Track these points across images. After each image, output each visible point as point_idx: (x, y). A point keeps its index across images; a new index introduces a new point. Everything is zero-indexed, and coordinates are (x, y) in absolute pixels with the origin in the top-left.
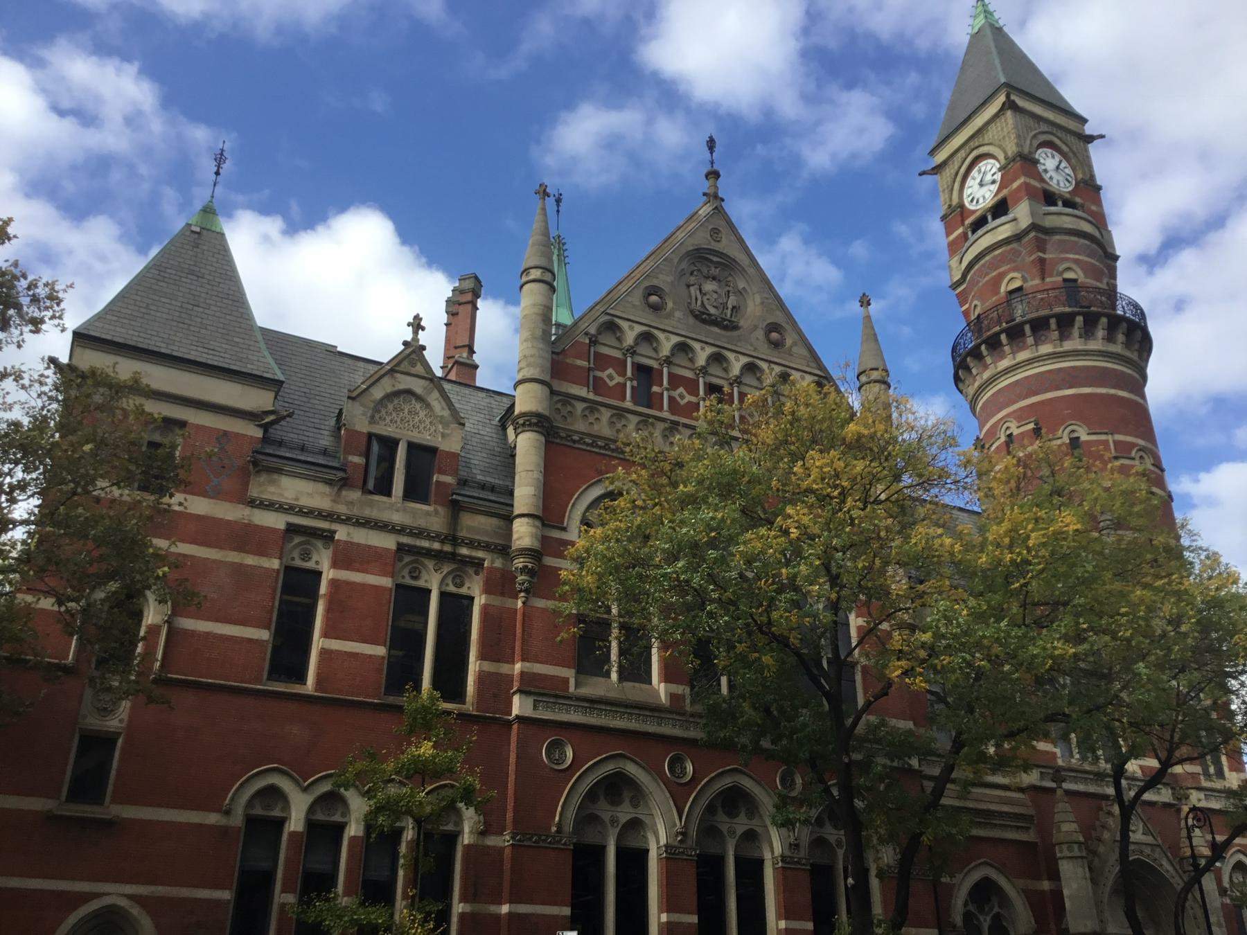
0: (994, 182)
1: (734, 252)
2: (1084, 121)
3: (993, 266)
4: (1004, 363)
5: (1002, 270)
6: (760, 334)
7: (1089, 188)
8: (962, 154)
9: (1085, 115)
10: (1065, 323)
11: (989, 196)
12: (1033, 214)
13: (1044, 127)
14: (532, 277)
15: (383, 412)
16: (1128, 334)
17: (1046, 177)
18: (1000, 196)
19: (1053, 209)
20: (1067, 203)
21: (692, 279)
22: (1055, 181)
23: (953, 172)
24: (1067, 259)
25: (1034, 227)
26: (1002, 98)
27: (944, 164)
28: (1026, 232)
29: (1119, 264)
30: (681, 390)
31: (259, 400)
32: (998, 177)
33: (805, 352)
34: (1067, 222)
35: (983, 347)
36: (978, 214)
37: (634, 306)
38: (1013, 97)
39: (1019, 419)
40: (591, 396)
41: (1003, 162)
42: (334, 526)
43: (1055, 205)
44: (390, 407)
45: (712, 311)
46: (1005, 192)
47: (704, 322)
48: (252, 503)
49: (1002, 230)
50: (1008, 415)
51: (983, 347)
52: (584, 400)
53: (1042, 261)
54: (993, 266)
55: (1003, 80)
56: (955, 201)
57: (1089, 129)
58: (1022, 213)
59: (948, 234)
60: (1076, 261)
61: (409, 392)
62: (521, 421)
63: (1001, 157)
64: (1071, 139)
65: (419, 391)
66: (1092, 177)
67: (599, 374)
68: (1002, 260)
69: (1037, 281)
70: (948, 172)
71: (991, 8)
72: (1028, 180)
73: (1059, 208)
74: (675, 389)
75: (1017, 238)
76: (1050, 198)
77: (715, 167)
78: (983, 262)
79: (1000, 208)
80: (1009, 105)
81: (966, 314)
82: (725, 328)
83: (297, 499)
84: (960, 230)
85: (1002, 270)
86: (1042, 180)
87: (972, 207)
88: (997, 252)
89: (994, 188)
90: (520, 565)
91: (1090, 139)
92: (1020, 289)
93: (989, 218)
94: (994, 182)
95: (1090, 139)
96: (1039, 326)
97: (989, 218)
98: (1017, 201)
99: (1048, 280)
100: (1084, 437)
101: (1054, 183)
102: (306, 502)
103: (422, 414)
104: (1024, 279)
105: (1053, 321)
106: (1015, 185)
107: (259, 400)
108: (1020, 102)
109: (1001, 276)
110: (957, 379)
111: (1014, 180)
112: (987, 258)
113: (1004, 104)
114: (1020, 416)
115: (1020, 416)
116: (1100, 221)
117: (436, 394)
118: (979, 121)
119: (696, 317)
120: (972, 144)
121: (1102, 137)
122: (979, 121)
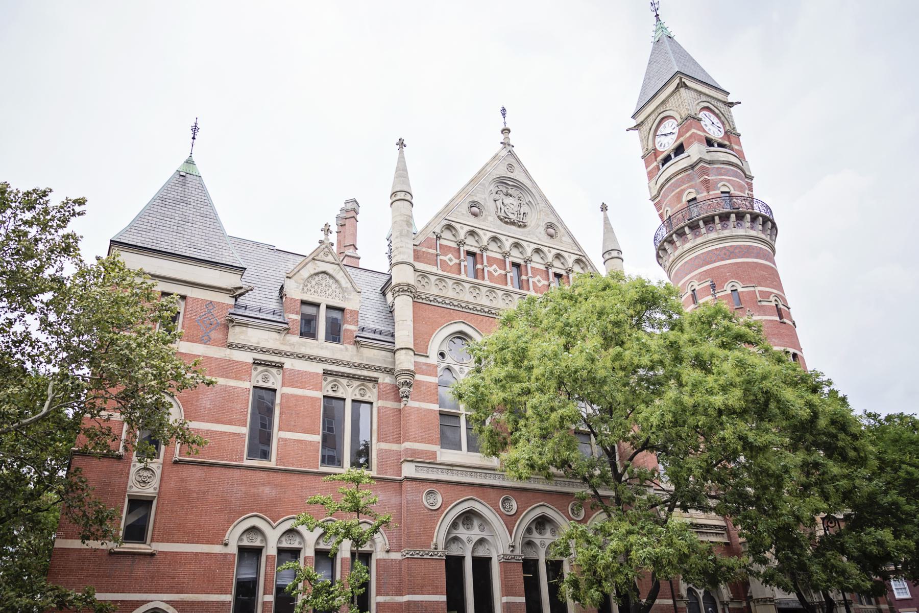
1: (522, 178)
3: (677, 185)
4: (688, 246)
6: (542, 229)
7: (732, 135)
8: (653, 117)
10: (725, 217)
11: (671, 142)
12: (700, 152)
13: (704, 98)
14: (398, 198)
15: (309, 286)
16: (764, 223)
17: (706, 129)
19: (712, 149)
20: (720, 145)
21: (497, 196)
23: (648, 128)
24: (722, 180)
26: (677, 81)
27: (642, 122)
28: (697, 163)
30: (495, 266)
31: (230, 280)
32: (676, 130)
33: (570, 241)
34: (723, 157)
35: (674, 236)
37: (463, 214)
38: (683, 80)
39: (699, 280)
40: (440, 272)
41: (679, 120)
42: (282, 360)
43: (713, 146)
44: (313, 282)
45: (511, 216)
46: (681, 139)
47: (506, 223)
48: (230, 346)
49: (681, 162)
50: (691, 278)
51: (674, 236)
52: (436, 275)
53: (707, 181)
54: (677, 185)
56: (650, 147)
57: (730, 99)
58: (695, 151)
59: (647, 167)
60: (729, 181)
61: (324, 273)
62: (397, 289)
63: (678, 117)
64: (720, 105)
65: (331, 272)
66: (734, 129)
67: (442, 257)
68: (682, 182)
69: (705, 194)
70: (645, 128)
71: (665, 25)
72: (695, 131)
73: (716, 148)
74: (491, 266)
76: (710, 142)
77: (508, 126)
78: (670, 183)
79: (679, 150)
81: (661, 216)
82: (520, 226)
83: (258, 343)
84: (655, 164)
86: (704, 131)
88: (679, 177)
89: (675, 137)
90: (402, 381)
91: (731, 105)
92: (695, 199)
93: (673, 156)
95: (731, 105)
96: (709, 221)
97: (673, 156)
98: (690, 144)
99: (711, 193)
101: (711, 132)
102: (264, 344)
103: (334, 286)
104: (698, 193)
105: (717, 218)
106: (688, 135)
107: (230, 280)
108: (688, 83)
109: (683, 191)
110: (658, 256)
111: (687, 131)
112: (673, 181)
114: (700, 278)
115: (700, 278)
116: (740, 155)
117: (342, 273)
118: (663, 96)
119: (501, 220)
120: (659, 111)
122: (663, 96)
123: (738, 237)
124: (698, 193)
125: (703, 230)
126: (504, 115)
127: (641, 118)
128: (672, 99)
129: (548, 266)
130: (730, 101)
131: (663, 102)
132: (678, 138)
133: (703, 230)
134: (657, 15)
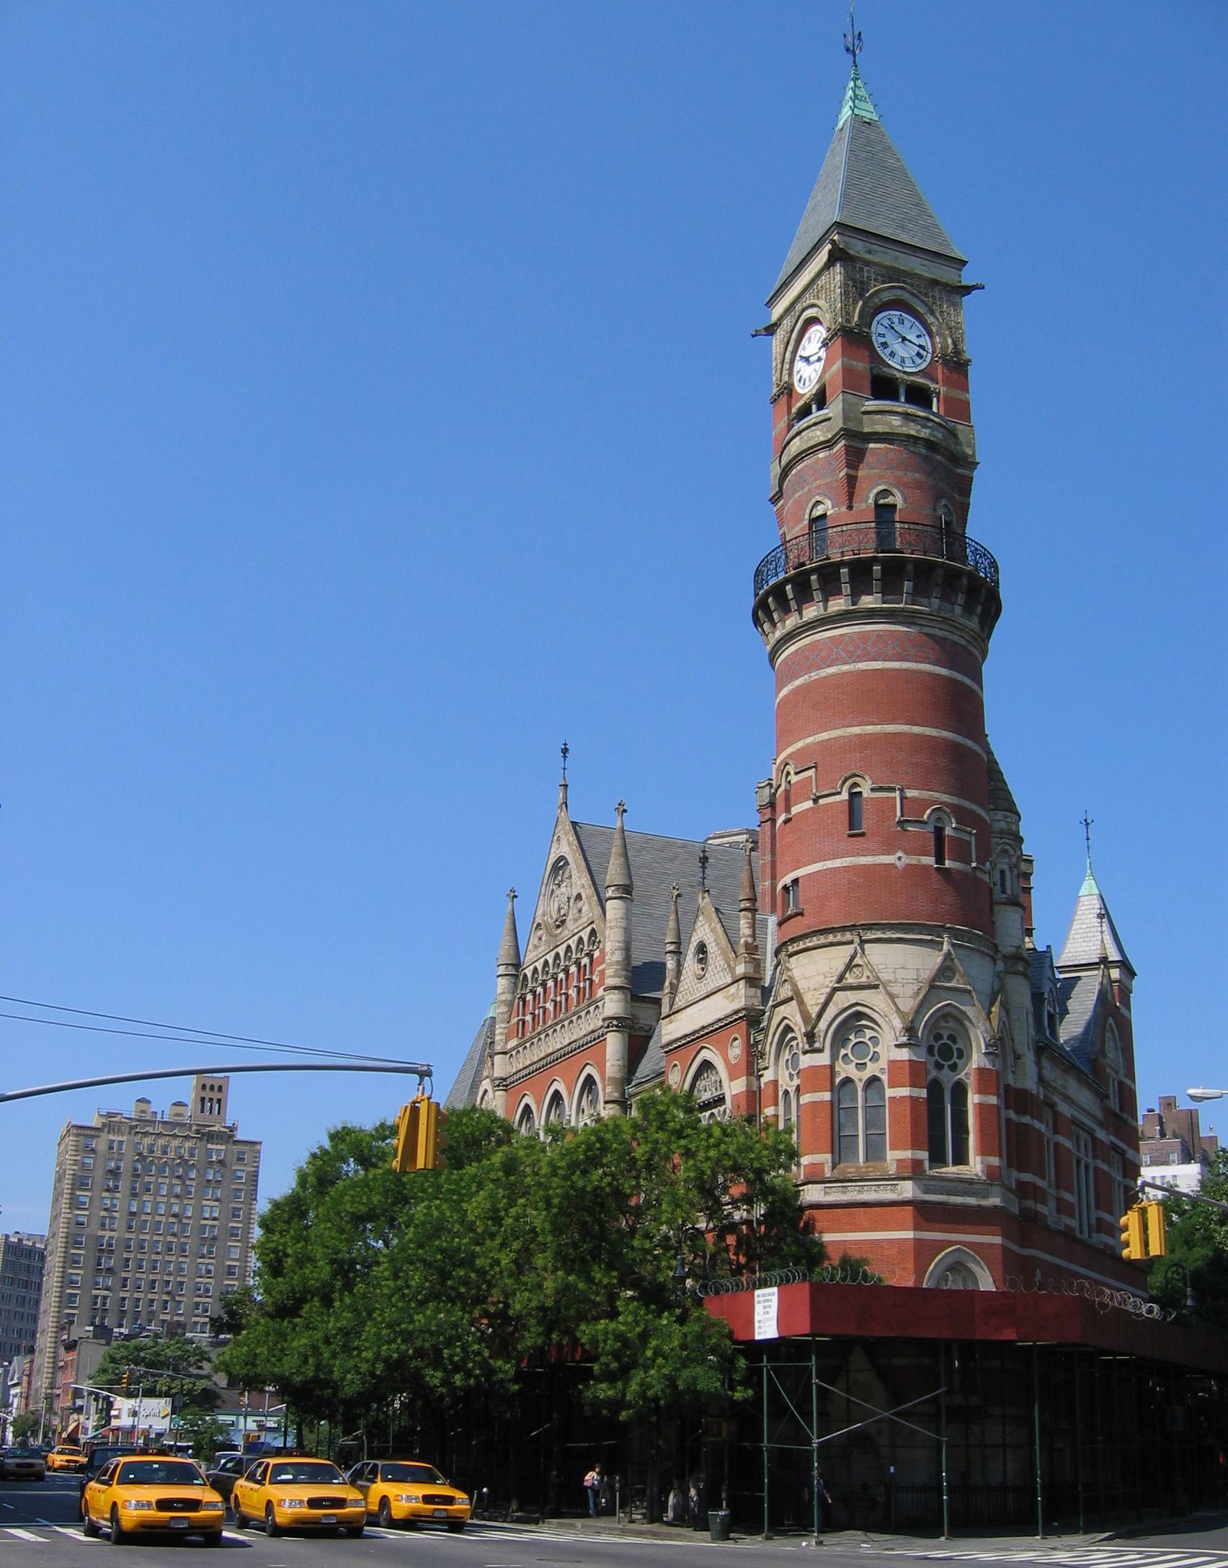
0: (819, 360)
11: (815, 378)
22: (897, 359)
25: (847, 433)
27: (781, 318)
29: (976, 474)
55: (836, 218)
57: (967, 278)
75: (828, 444)
80: (838, 255)
87: (800, 391)
89: (819, 366)
93: (814, 407)
94: (819, 360)
97: (814, 407)
113: (830, 251)
130: (964, 283)
132: (824, 371)
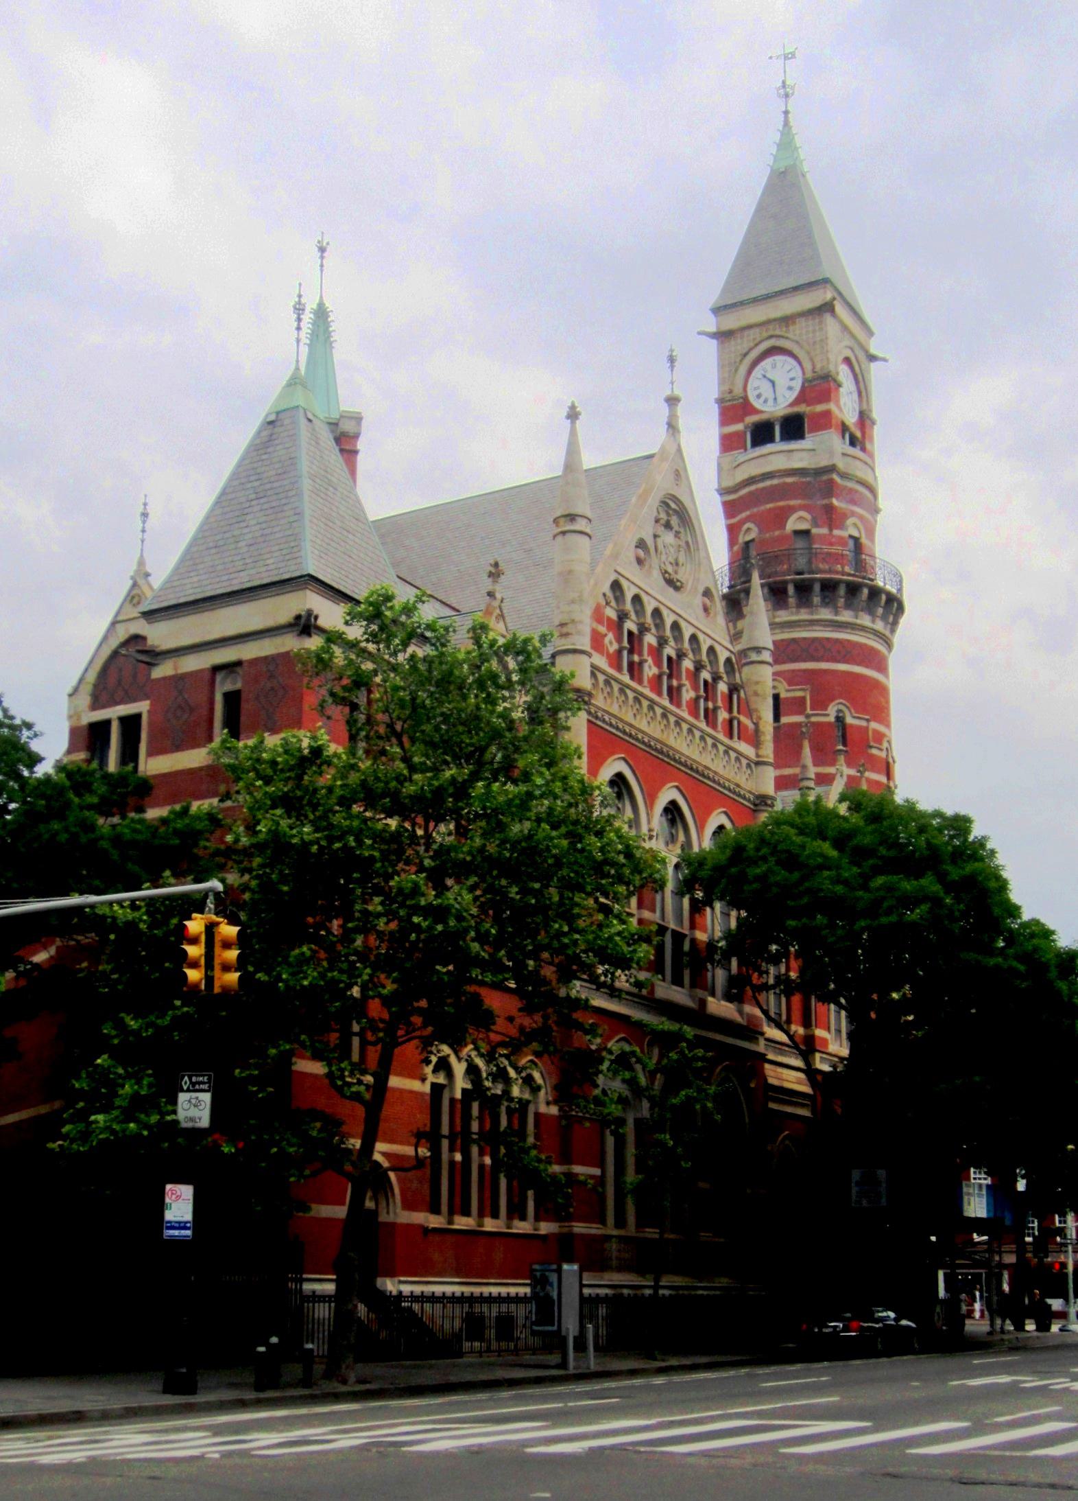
2: (870, 333)
5: (792, 503)
8: (755, 334)
9: (874, 329)
18: (796, 409)
29: (879, 518)
36: (763, 417)
46: (802, 408)
56: (738, 391)
85: (792, 503)
87: (757, 404)
92: (806, 533)
95: (873, 358)
100: (849, 720)
109: (792, 510)
121: (885, 360)
123: (863, 628)
124: (816, 525)
125: (816, 600)
126: (672, 367)
127: (732, 321)
128: (802, 322)
129: (699, 667)
130: (873, 351)
131: (787, 320)
133: (816, 600)
134: (786, 113)
